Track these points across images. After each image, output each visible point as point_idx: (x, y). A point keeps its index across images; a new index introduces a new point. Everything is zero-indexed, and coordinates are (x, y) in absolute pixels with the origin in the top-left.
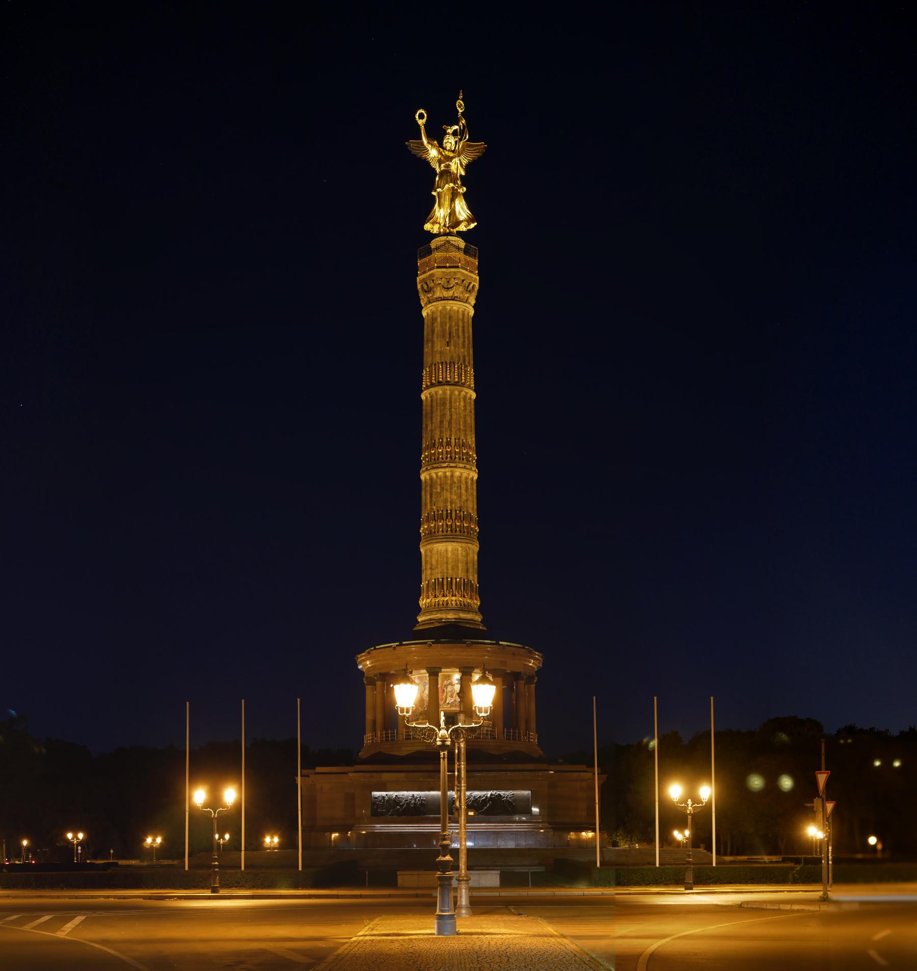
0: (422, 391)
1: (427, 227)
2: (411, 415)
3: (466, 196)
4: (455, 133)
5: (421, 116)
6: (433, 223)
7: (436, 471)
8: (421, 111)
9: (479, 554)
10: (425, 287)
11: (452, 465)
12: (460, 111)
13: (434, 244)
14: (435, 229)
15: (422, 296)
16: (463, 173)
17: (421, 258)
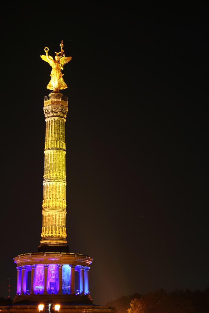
0: (44, 150)
1: (48, 87)
2: (41, 159)
3: (63, 77)
4: (59, 55)
5: (47, 49)
6: (51, 87)
7: (50, 182)
8: (47, 48)
9: (66, 215)
10: (47, 111)
11: (55, 180)
12: (62, 47)
13: (50, 95)
14: (51, 89)
15: (45, 115)
16: (63, 69)
17: (45, 100)
